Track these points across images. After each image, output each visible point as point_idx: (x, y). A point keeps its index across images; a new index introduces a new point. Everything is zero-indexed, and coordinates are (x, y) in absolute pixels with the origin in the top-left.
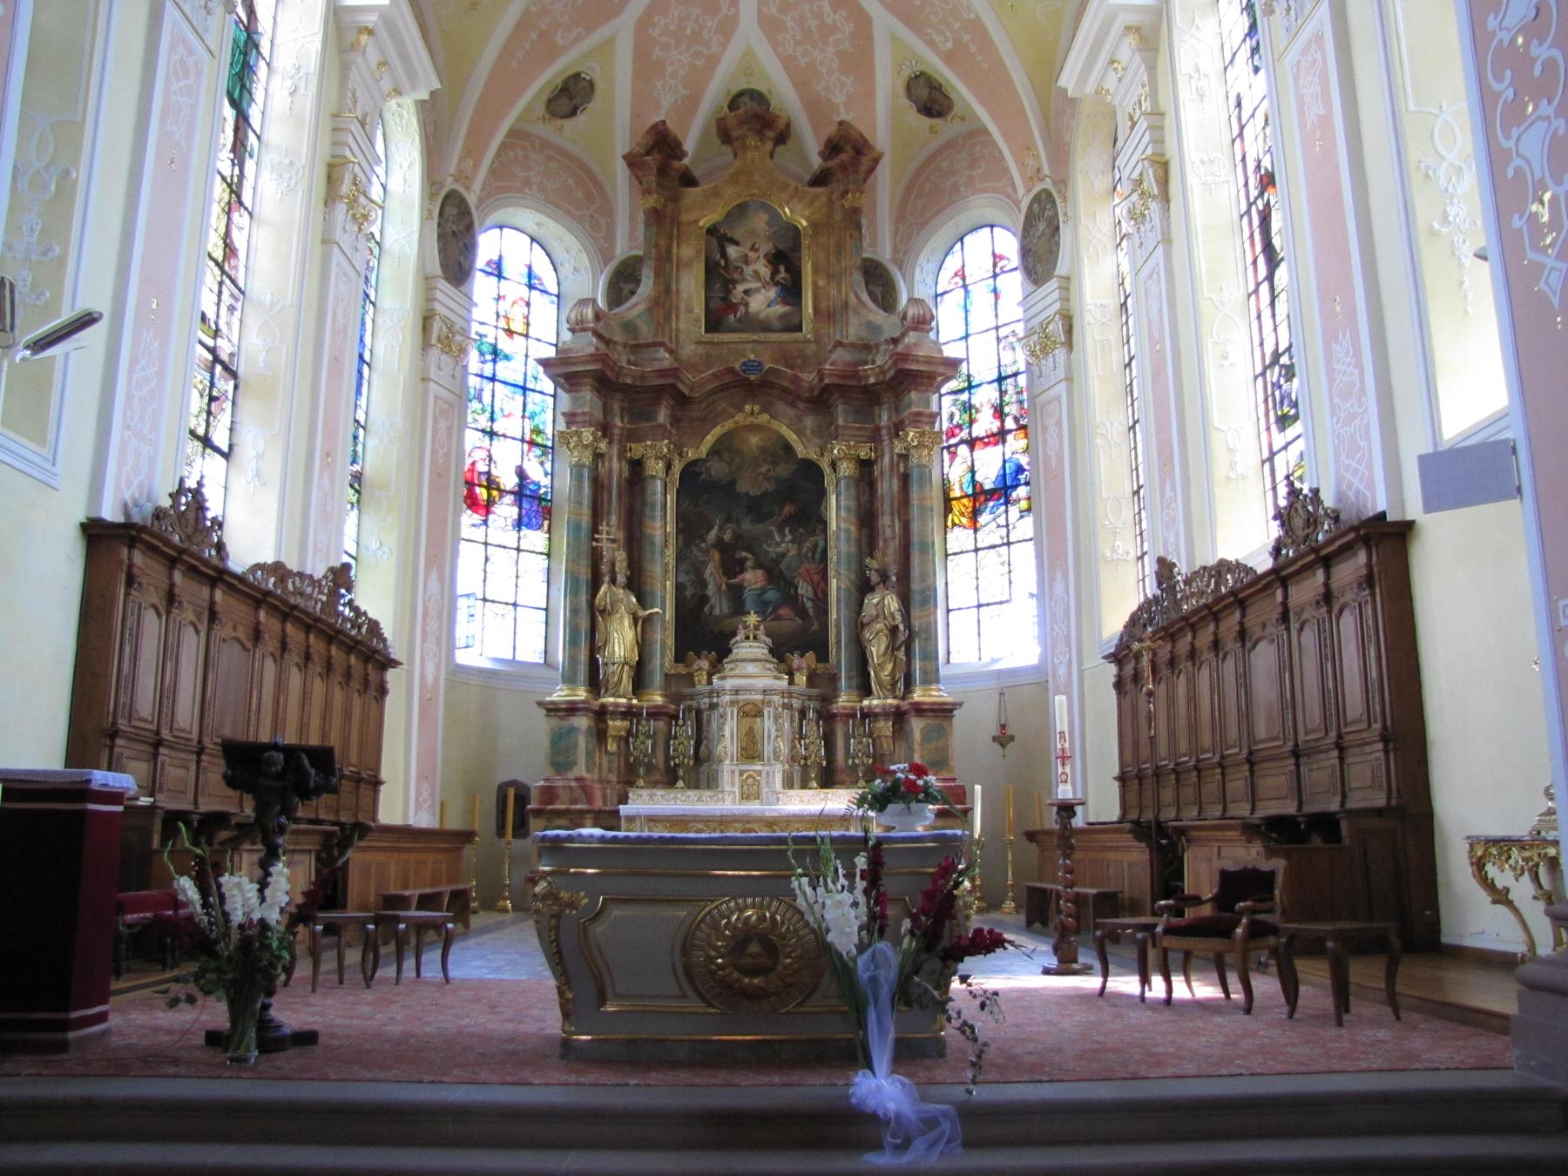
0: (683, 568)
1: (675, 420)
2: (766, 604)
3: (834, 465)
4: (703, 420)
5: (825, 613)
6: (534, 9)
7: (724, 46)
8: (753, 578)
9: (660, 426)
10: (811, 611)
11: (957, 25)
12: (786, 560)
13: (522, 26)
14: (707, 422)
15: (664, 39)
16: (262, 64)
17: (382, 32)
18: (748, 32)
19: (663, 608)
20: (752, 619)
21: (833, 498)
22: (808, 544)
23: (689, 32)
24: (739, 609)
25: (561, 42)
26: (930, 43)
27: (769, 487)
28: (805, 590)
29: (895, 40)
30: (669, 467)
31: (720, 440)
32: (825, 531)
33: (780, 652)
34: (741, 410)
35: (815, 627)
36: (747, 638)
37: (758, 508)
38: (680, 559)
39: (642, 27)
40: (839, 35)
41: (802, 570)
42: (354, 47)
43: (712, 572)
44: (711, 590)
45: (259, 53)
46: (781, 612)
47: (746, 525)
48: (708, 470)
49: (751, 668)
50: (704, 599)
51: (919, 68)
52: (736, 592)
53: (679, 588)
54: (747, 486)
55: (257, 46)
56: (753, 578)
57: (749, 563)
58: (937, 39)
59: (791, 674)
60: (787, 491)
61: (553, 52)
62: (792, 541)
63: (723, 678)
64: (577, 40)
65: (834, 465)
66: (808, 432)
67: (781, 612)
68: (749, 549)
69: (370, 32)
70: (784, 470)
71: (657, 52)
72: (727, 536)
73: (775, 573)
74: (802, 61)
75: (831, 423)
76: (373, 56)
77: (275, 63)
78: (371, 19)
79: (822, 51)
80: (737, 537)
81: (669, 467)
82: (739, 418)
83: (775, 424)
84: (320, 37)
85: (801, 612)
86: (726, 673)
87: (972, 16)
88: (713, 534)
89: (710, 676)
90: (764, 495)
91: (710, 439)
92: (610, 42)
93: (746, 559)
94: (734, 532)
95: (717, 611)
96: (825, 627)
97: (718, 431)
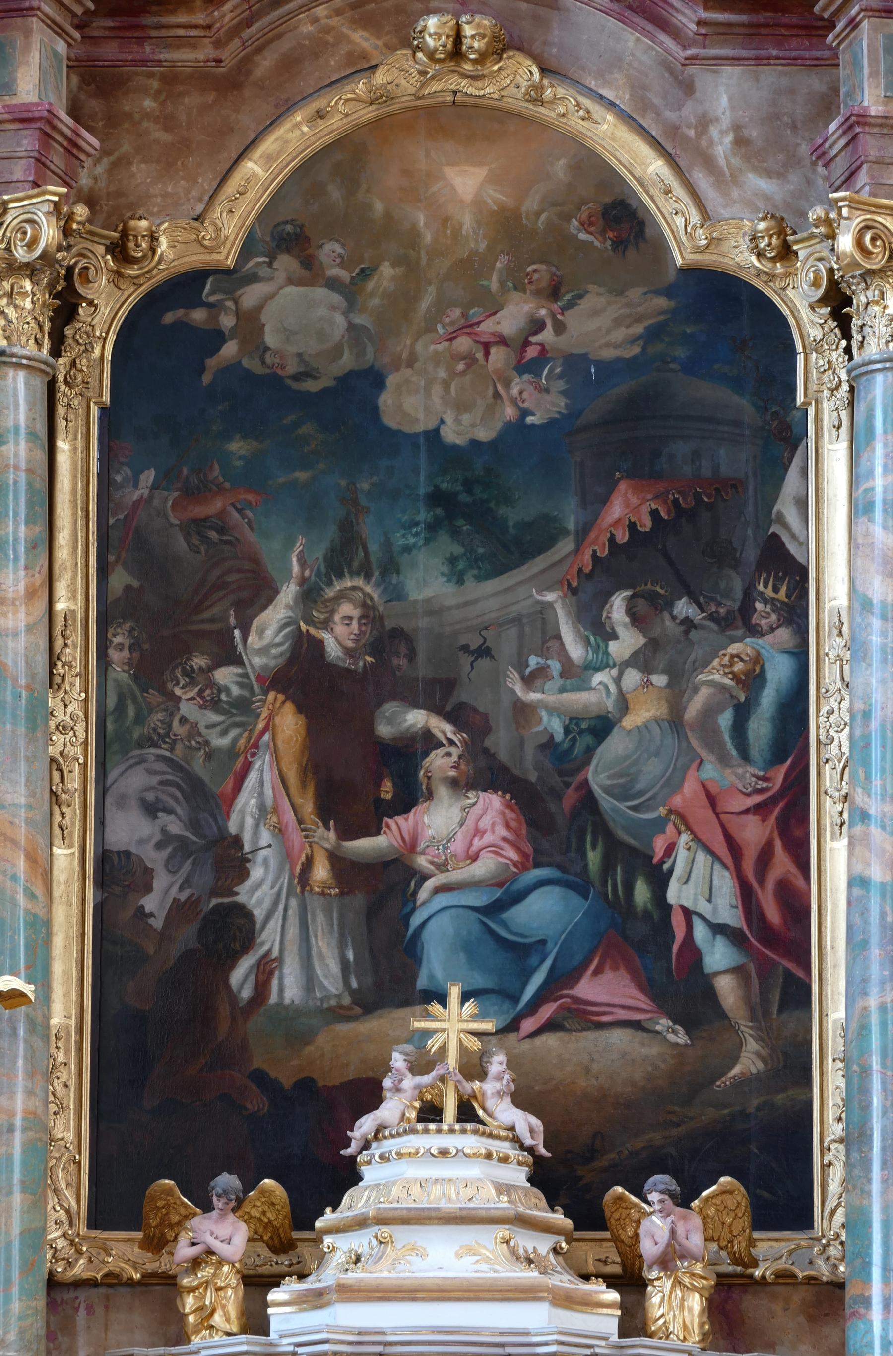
0: (134, 781)
1: (95, 83)
2: (521, 952)
3: (837, 302)
4: (229, 83)
5: (797, 995)
8: (457, 831)
9: (24, 118)
10: (727, 989)
12: (615, 746)
14: (240, 92)
19: (40, 972)
20: (454, 1024)
21: (834, 457)
22: (715, 675)
24: (391, 977)
27: (543, 404)
28: (700, 888)
30: (65, 307)
31: (306, 175)
32: (795, 614)
33: (577, 1178)
34: (407, 39)
35: (750, 1061)
36: (430, 1113)
37: (479, 503)
38: (112, 744)
41: (688, 793)
43: (265, 805)
44: (260, 888)
46: (588, 989)
47: (428, 582)
48: (250, 325)
49: (442, 1255)
50: (230, 930)
52: (380, 898)
53: (114, 875)
54: (431, 399)
56: (457, 831)
57: (439, 764)
59: (630, 1282)
60: (623, 422)
62: (642, 661)
63: (316, 1300)
65: (837, 302)
66: (722, 146)
67: (588, 989)
68: (441, 696)
70: (603, 325)
72: (337, 640)
73: (558, 808)
75: (828, 104)
80: (385, 638)
81: (65, 307)
82: (400, 76)
83: (565, 107)
85: (682, 991)
86: (328, 1275)
88: (268, 633)
89: (257, 1284)
90: (518, 430)
91: (259, 173)
93: (429, 741)
94: (369, 614)
95: (289, 987)
96: (793, 1064)
97: (294, 138)
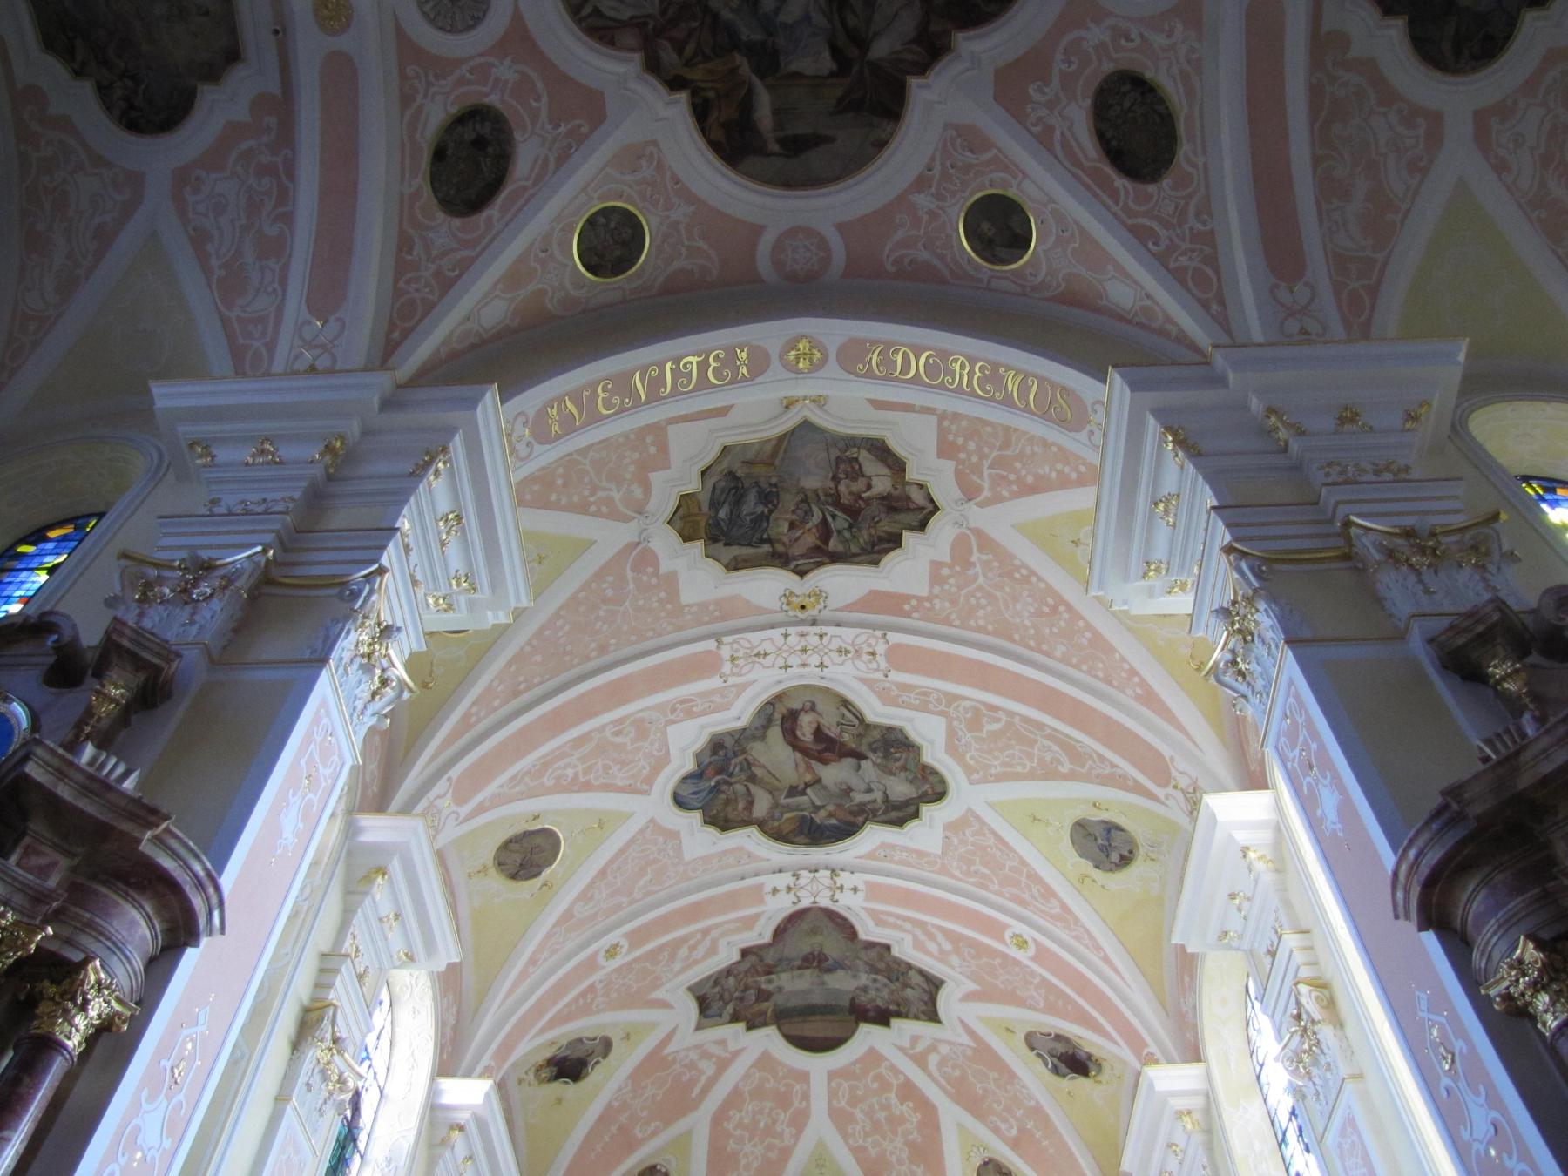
6: (616, 1104)
7: (797, 1137)
11: (1020, 1113)
13: (604, 1119)
15: (738, 1132)
16: (357, 1157)
17: (473, 1129)
18: (820, 1127)
23: (762, 1125)
25: (640, 1136)
26: (996, 1131)
29: (960, 1126)
39: (719, 1118)
40: (908, 1126)
42: (445, 1142)
45: (355, 1146)
51: (987, 1155)
55: (355, 1140)
58: (1003, 1126)
61: (631, 1145)
64: (654, 1134)
69: (461, 1128)
71: (731, 1145)
74: (873, 1152)
76: (460, 1150)
77: (368, 1156)
78: (463, 1117)
79: (892, 1141)
84: (414, 1132)
87: (1033, 1103)
92: (689, 1133)
